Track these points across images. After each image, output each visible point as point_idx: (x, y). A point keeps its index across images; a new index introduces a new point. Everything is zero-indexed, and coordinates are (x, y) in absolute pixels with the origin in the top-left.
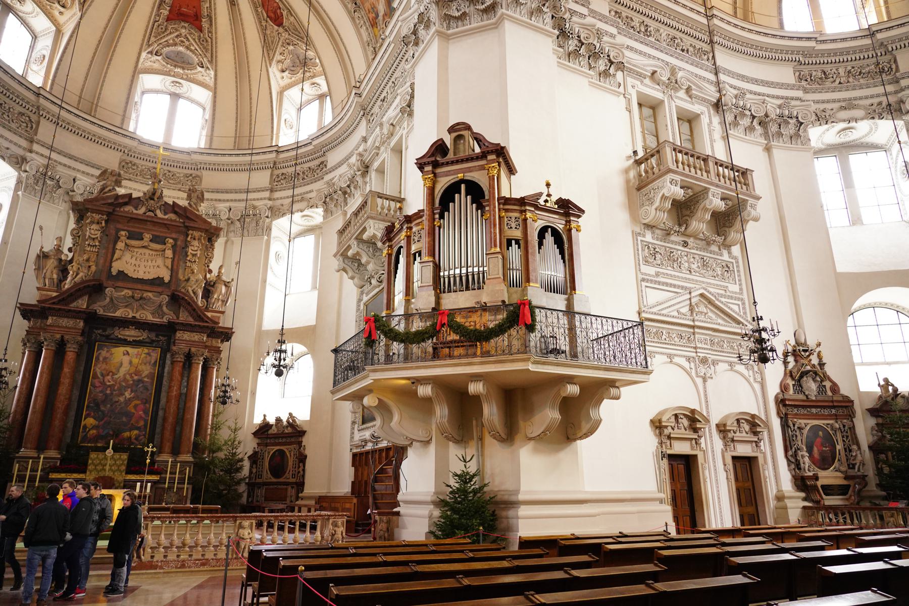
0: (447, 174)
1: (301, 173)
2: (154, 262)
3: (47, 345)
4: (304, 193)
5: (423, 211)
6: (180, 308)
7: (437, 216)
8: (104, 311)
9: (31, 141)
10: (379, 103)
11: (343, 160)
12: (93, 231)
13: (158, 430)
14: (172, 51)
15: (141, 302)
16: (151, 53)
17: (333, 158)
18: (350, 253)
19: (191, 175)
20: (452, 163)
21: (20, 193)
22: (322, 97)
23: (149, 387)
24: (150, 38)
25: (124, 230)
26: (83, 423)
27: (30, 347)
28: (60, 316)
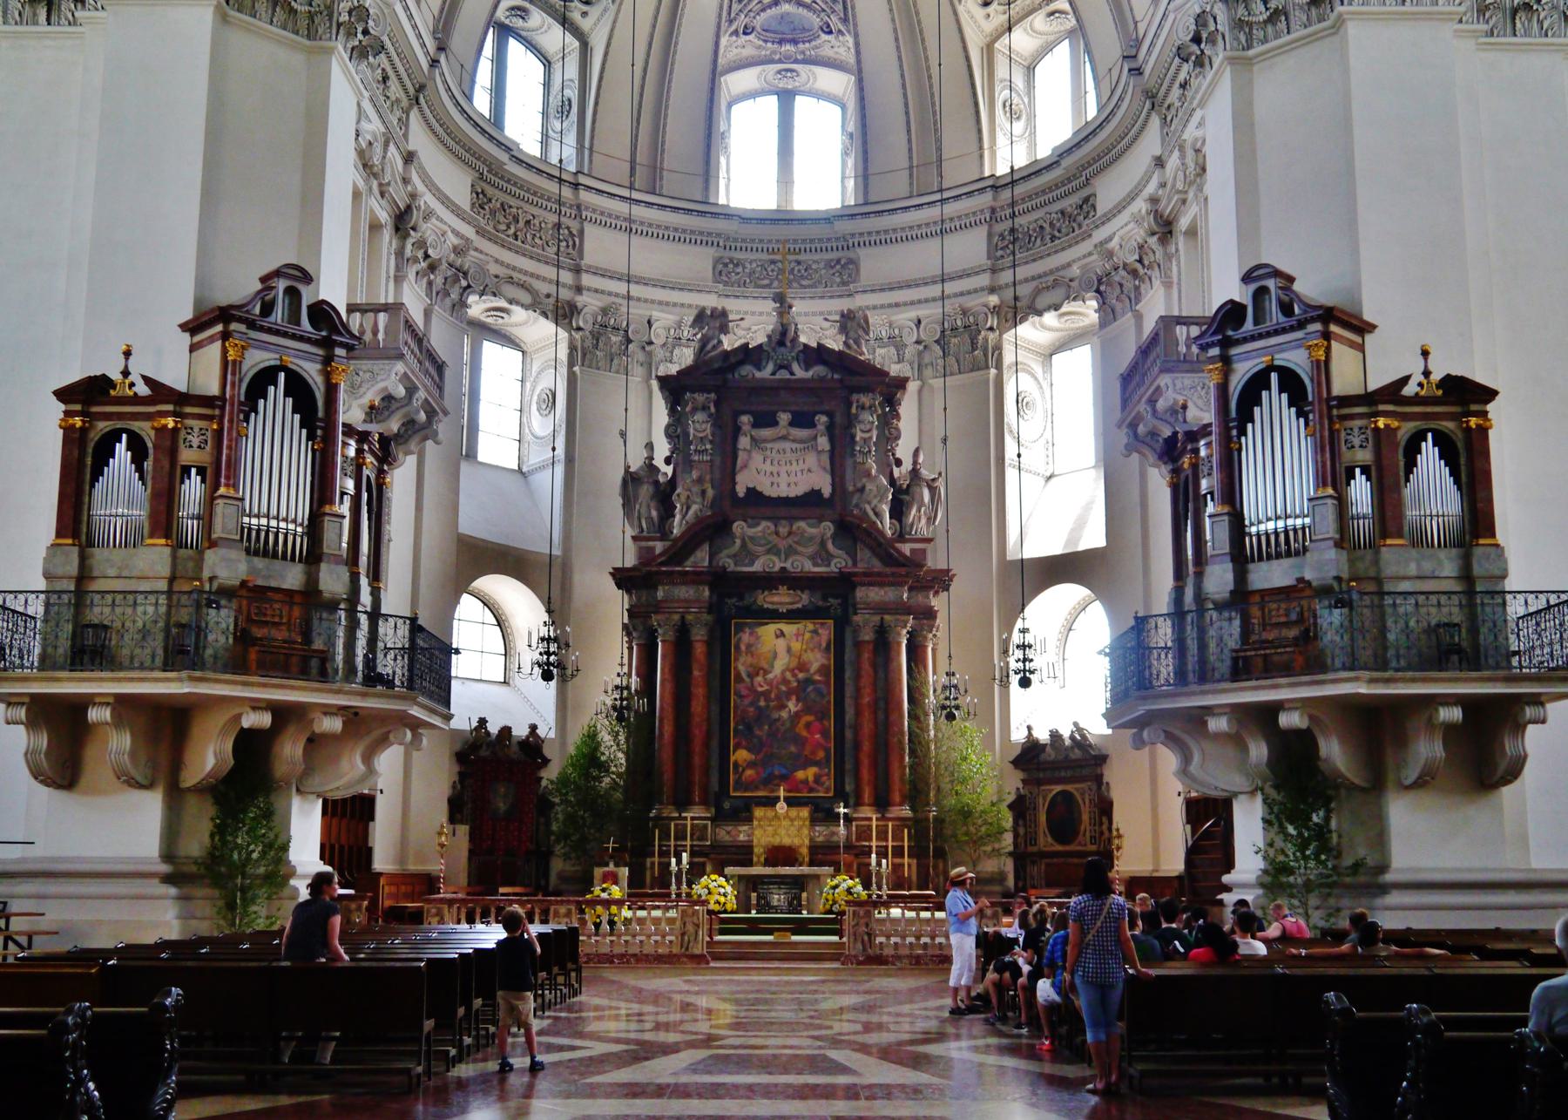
0: (1247, 356)
1: (1046, 226)
2: (801, 462)
3: (664, 635)
4: (1058, 269)
5: (1210, 425)
6: (855, 542)
7: (1234, 432)
8: (736, 565)
9: (577, 270)
10: (1176, 92)
11: (1124, 199)
12: (699, 425)
13: (848, 766)
14: (772, 17)
15: (790, 541)
16: (736, 33)
17: (1109, 190)
18: (1141, 429)
19: (838, 261)
20: (1253, 338)
21: (576, 369)
22: (1070, 34)
23: (825, 692)
24: (730, 7)
25: (744, 413)
26: (732, 758)
27: (639, 638)
28: (674, 584)
